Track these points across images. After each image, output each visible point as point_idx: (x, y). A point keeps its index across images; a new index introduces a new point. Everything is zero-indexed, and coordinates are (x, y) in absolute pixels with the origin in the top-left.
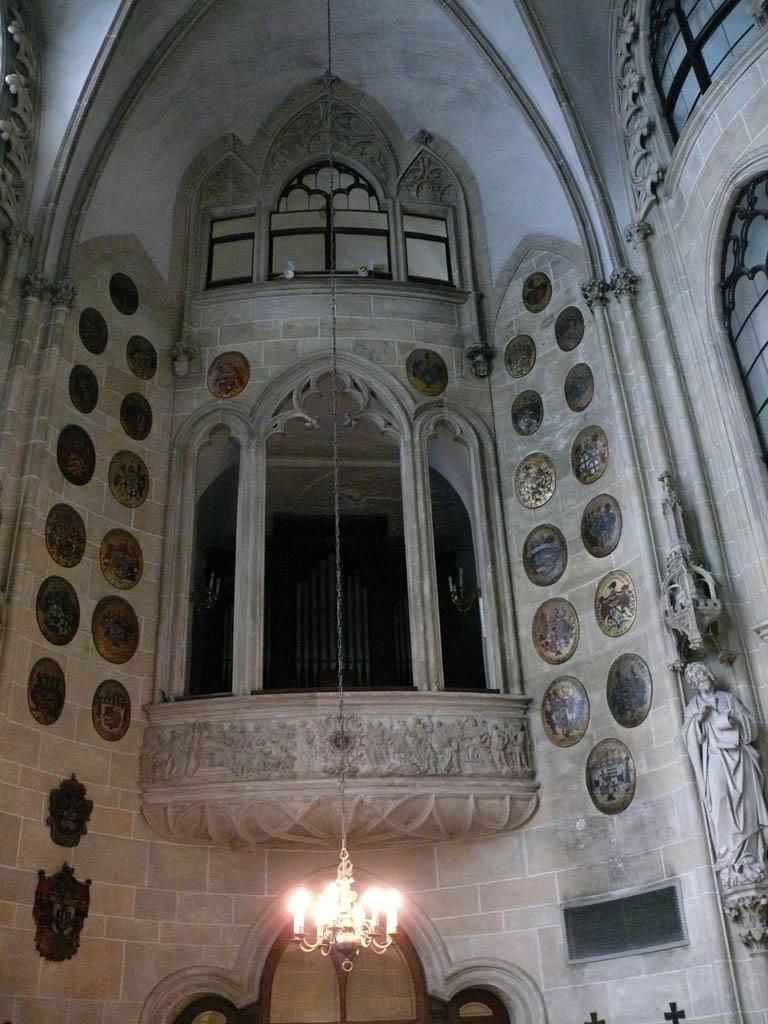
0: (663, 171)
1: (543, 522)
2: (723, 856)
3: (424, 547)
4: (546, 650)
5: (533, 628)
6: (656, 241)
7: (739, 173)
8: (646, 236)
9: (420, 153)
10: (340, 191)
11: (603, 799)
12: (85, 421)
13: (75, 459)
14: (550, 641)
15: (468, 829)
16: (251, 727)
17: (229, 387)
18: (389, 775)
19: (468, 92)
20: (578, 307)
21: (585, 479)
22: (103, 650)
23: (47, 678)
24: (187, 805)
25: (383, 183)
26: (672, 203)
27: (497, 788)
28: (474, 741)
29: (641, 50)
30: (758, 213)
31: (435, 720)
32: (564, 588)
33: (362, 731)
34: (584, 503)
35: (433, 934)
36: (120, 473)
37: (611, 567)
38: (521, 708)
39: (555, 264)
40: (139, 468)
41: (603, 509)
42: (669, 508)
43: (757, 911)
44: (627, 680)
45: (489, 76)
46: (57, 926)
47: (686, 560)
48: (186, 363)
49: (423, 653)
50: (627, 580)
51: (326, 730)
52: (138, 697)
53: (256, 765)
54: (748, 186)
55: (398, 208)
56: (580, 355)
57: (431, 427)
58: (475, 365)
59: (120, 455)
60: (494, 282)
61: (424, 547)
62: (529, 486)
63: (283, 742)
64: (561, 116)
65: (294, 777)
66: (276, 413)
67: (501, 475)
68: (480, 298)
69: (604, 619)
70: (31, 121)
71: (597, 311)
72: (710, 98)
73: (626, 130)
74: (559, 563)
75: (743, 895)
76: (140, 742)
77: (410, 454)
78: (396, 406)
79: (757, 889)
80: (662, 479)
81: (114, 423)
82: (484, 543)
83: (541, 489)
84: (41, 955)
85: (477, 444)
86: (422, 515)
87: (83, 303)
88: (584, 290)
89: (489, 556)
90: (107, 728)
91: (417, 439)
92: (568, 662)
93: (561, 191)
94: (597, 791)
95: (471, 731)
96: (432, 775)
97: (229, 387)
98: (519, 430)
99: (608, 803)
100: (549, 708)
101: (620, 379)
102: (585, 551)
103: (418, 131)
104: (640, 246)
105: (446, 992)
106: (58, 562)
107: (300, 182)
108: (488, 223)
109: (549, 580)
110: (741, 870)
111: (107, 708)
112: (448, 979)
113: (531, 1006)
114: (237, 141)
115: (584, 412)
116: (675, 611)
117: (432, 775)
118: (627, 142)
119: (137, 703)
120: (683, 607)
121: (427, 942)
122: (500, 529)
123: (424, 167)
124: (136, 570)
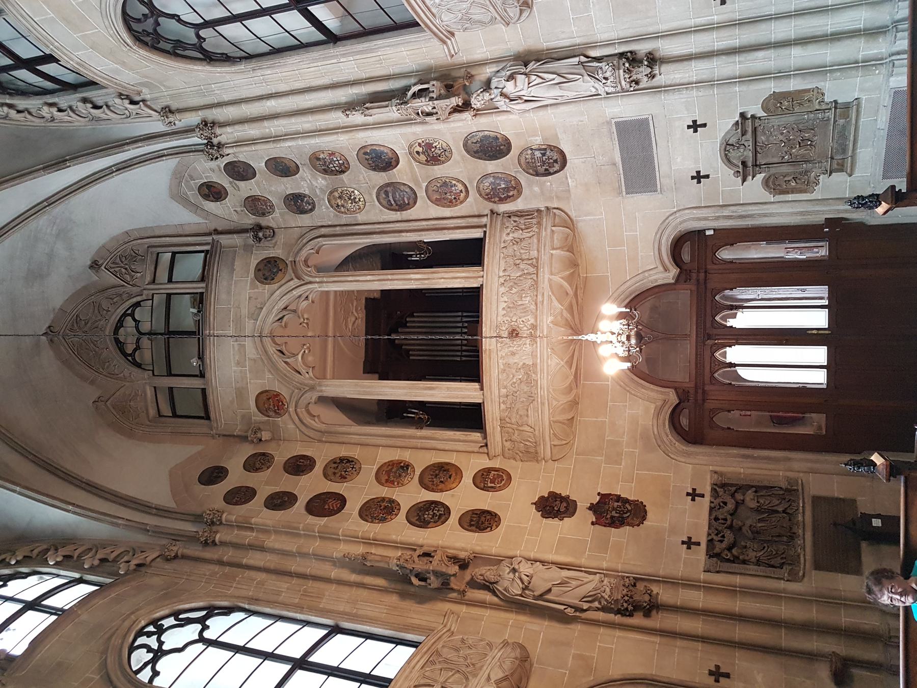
0: (120, 95)
2: (597, 89)
3: (390, 277)
5: (444, 207)
6: (174, 105)
7: (125, 42)
8: (171, 112)
11: (557, 167)
13: (329, 505)
14: (453, 197)
15: (571, 254)
16: (504, 391)
17: (280, 404)
18: (536, 304)
22: (454, 485)
23: (472, 520)
24: (552, 432)
25: (131, 296)
27: (546, 235)
28: (515, 249)
29: (21, 103)
30: (155, 30)
31: (501, 274)
32: (420, 187)
37: (406, 153)
38: (496, 217)
39: (192, 178)
41: (367, 157)
42: (367, 112)
43: (633, 69)
44: (480, 147)
45: (45, 217)
47: (402, 103)
49: (459, 280)
52: (484, 463)
54: (134, 36)
55: (149, 287)
56: (259, 165)
57: (309, 269)
59: (326, 475)
61: (390, 277)
62: (350, 205)
65: (534, 365)
66: (299, 373)
68: (217, 232)
73: (87, 119)
74: (402, 188)
75: (622, 78)
76: (512, 461)
77: (327, 284)
78: (294, 292)
79: (619, 69)
83: (352, 198)
84: (643, 523)
85: (321, 239)
86: (369, 278)
87: (220, 504)
88: (212, 159)
89: (396, 234)
90: (503, 482)
91: (317, 280)
95: (510, 251)
96: (537, 277)
97: (280, 404)
98: (312, 210)
101: (277, 138)
102: (394, 170)
103: (89, 270)
104: (178, 116)
105: (674, 271)
106: (396, 515)
107: (130, 355)
110: (606, 79)
112: (666, 270)
115: (300, 166)
116: (437, 113)
117: (537, 277)
118: (98, 119)
119: (488, 464)
120: (434, 108)
124: (402, 464)
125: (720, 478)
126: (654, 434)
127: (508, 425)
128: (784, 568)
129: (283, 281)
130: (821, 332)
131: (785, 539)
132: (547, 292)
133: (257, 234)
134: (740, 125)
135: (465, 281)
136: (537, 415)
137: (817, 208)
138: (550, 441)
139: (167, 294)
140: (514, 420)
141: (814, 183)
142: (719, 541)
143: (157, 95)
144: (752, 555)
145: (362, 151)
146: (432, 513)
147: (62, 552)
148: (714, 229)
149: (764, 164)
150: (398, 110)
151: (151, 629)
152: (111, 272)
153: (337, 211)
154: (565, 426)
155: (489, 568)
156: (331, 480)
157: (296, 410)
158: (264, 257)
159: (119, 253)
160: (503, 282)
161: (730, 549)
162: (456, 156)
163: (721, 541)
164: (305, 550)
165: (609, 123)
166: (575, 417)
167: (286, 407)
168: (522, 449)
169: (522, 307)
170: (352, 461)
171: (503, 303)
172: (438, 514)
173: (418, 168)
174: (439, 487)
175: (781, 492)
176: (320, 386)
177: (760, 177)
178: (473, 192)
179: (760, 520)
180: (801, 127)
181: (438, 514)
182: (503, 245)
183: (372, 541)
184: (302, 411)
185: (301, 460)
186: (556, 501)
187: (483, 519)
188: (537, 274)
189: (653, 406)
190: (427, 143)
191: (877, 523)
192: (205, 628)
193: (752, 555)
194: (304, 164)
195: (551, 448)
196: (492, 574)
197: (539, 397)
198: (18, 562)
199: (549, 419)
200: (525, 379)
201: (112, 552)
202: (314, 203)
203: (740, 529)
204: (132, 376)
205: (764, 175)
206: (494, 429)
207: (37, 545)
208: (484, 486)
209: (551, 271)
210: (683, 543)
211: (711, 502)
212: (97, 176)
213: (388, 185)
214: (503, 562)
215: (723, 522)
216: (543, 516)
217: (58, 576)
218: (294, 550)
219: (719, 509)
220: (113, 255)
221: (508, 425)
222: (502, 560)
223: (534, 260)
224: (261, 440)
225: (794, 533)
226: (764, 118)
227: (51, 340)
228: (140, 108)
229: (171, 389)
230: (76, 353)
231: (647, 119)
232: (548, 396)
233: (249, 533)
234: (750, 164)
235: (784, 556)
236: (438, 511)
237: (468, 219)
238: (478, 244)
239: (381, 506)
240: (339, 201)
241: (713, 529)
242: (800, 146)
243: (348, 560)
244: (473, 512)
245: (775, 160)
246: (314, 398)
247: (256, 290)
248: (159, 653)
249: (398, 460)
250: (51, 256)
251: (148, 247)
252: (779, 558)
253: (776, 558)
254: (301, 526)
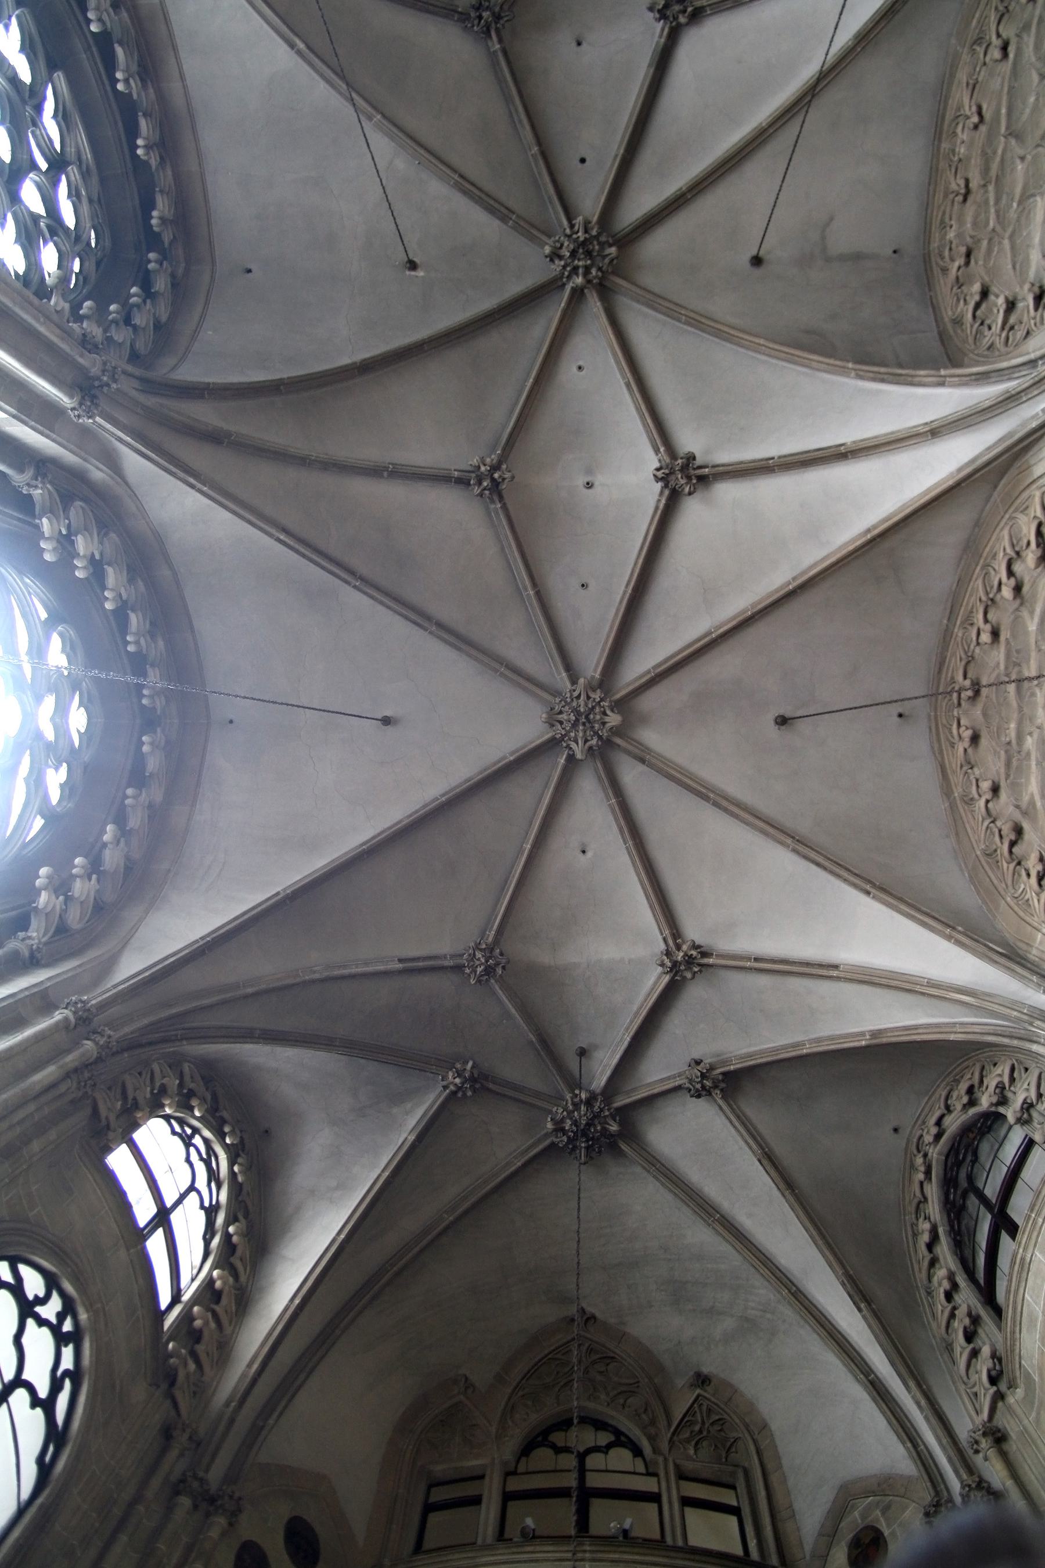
6: (1013, 1446)
10: (596, 1449)
19: (747, 1319)
25: (652, 1439)
26: (1020, 1392)
29: (944, 1249)
39: (886, 1509)
45: (772, 1297)
64: (863, 1325)
70: (230, 1323)
72: (1026, 1236)
73: (945, 1336)
87: (248, 1529)
103: (692, 1373)
104: (992, 1453)
108: (791, 1482)
114: (468, 1384)
118: (949, 1348)
123: (702, 1417)
143: (1019, 1411)
151: (67, 1326)
192: (36, 1402)
220: (723, 1406)
227: (573, 1320)
230: (550, 1356)
248: (27, 1309)
250: (712, 1312)
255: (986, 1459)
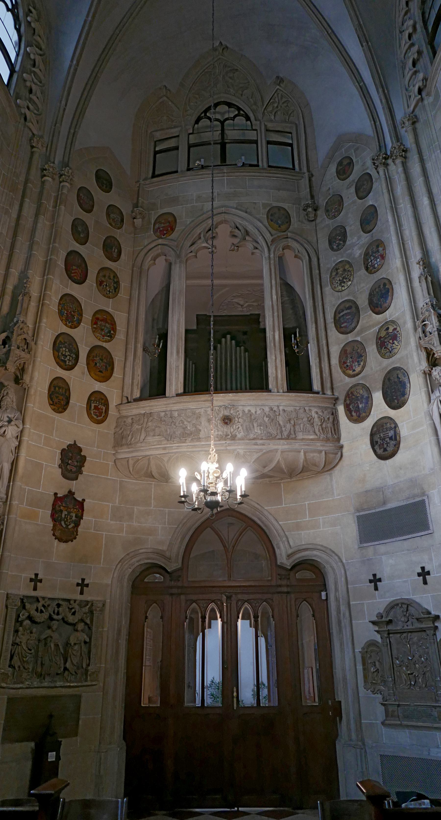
0: (425, 79)
1: (346, 298)
3: (276, 314)
4: (347, 369)
5: (340, 357)
8: (414, 123)
9: (276, 91)
11: (380, 452)
12: (81, 249)
13: (76, 269)
14: (349, 364)
16: (176, 414)
17: (165, 232)
18: (254, 439)
20: (369, 172)
21: (371, 271)
22: (93, 375)
23: (59, 388)
26: (431, 99)
28: (304, 420)
31: (281, 408)
33: (239, 414)
34: (370, 286)
35: (280, 531)
36: (103, 279)
37: (387, 319)
40: (114, 277)
41: (382, 286)
42: (423, 278)
44: (395, 382)
46: (65, 523)
47: (434, 307)
48: (140, 220)
49: (274, 372)
50: (396, 325)
51: (218, 414)
52: (113, 401)
53: (178, 435)
55: (263, 127)
56: (370, 201)
57: (281, 249)
58: (307, 215)
59: (102, 269)
60: (319, 167)
62: (338, 279)
63: (194, 422)
66: (191, 245)
67: (322, 275)
68: (311, 176)
69: (381, 349)
71: (381, 170)
74: (355, 320)
76: (115, 425)
77: (268, 264)
78: (260, 238)
80: (418, 263)
81: (99, 252)
82: (311, 313)
83: (345, 280)
84: (55, 539)
85: (307, 257)
86: (275, 297)
88: (373, 159)
89: (313, 319)
90: (95, 417)
91: (272, 256)
92: (360, 376)
93: (360, 101)
94: (376, 447)
97: (165, 232)
98: (332, 249)
99: (384, 453)
100: (348, 402)
101: (394, 209)
102: (371, 312)
104: (410, 129)
105: (288, 564)
106: (66, 325)
107: (205, 115)
109: (348, 330)
111: (95, 406)
112: (289, 556)
113: (337, 571)
115: (371, 233)
116: (426, 336)
117: (279, 439)
118: (403, 68)
119: (112, 405)
120: (431, 333)
121: (277, 536)
122: (320, 304)
123: (279, 100)
124: (112, 332)
125: (98, 609)
126: (139, 550)
127: (146, 420)
128: (10, 669)
129: (270, 229)
130: (235, 700)
131: (39, 670)
132: (266, 448)
133: (310, 207)
134: (428, 616)
135: (273, 377)
136: (155, 444)
137: (350, 692)
138: (131, 457)
139: (257, 140)
140: (150, 424)
141: (374, 689)
142: (37, 608)
144: (23, 638)
145: (387, 282)
146: (67, 354)
147: (38, 59)
148: (327, 599)
149: (390, 642)
150: (427, 304)
152: (274, 94)
153: (332, 269)
154: (145, 469)
155: (15, 400)
156: (99, 273)
157: (160, 244)
158: (290, 213)
159: (290, 100)
160: (274, 410)
161: (30, 618)
162: (386, 362)
163: (37, 610)
164: (35, 247)
165: (423, 494)
166: (155, 480)
167: (163, 237)
168: (125, 433)
169: (252, 427)
170: (115, 291)
171: (255, 410)
172: (66, 359)
173: (374, 331)
174: (91, 362)
175: (84, 666)
176: (180, 262)
177: (378, 638)
178: (354, 381)
179: (57, 645)
180: (428, 674)
181: (66, 359)
182: (307, 408)
183: (41, 303)
184: (159, 250)
185: (116, 250)
186: (77, 462)
187: (61, 397)
188: (281, 439)
189: (165, 548)
190: (397, 335)
191: (52, 756)
193: (23, 638)
194: (372, 236)
195: (125, 458)
196: (8, 403)
197: (171, 445)
198: (29, 23)
199: (151, 455)
200: (186, 432)
201: (38, 98)
202: (338, 250)
203: (49, 627)
204: (188, 117)
205: (379, 640)
206: (143, 407)
207: (45, 41)
208: (92, 400)
209: (285, 451)
210: (36, 575)
211: (75, 601)
212: (355, 71)
213: (357, 308)
214: (19, 413)
215: (56, 611)
216: (63, 450)
217: (18, 55)
218: (35, 239)
219: (69, 608)
221: (146, 420)
222: (21, 413)
223: (294, 436)
224: (134, 218)
225: (44, 679)
226: (435, 639)
228: (415, 96)
229: (177, 148)
231: (428, 528)
232: (172, 453)
233: (52, 203)
234: (390, 627)
235: (22, 668)
236: (69, 360)
237: (329, 379)
238: (309, 389)
239: (74, 312)
240: (342, 269)
241: (48, 602)
242: (409, 674)
243: (25, 281)
244: (68, 390)
245: (395, 652)
246: (170, 258)
247: (261, 208)
249: (116, 329)
251: (296, 124)
252: (19, 664)
253: (20, 661)
254: (57, 245)
255: (406, 131)
